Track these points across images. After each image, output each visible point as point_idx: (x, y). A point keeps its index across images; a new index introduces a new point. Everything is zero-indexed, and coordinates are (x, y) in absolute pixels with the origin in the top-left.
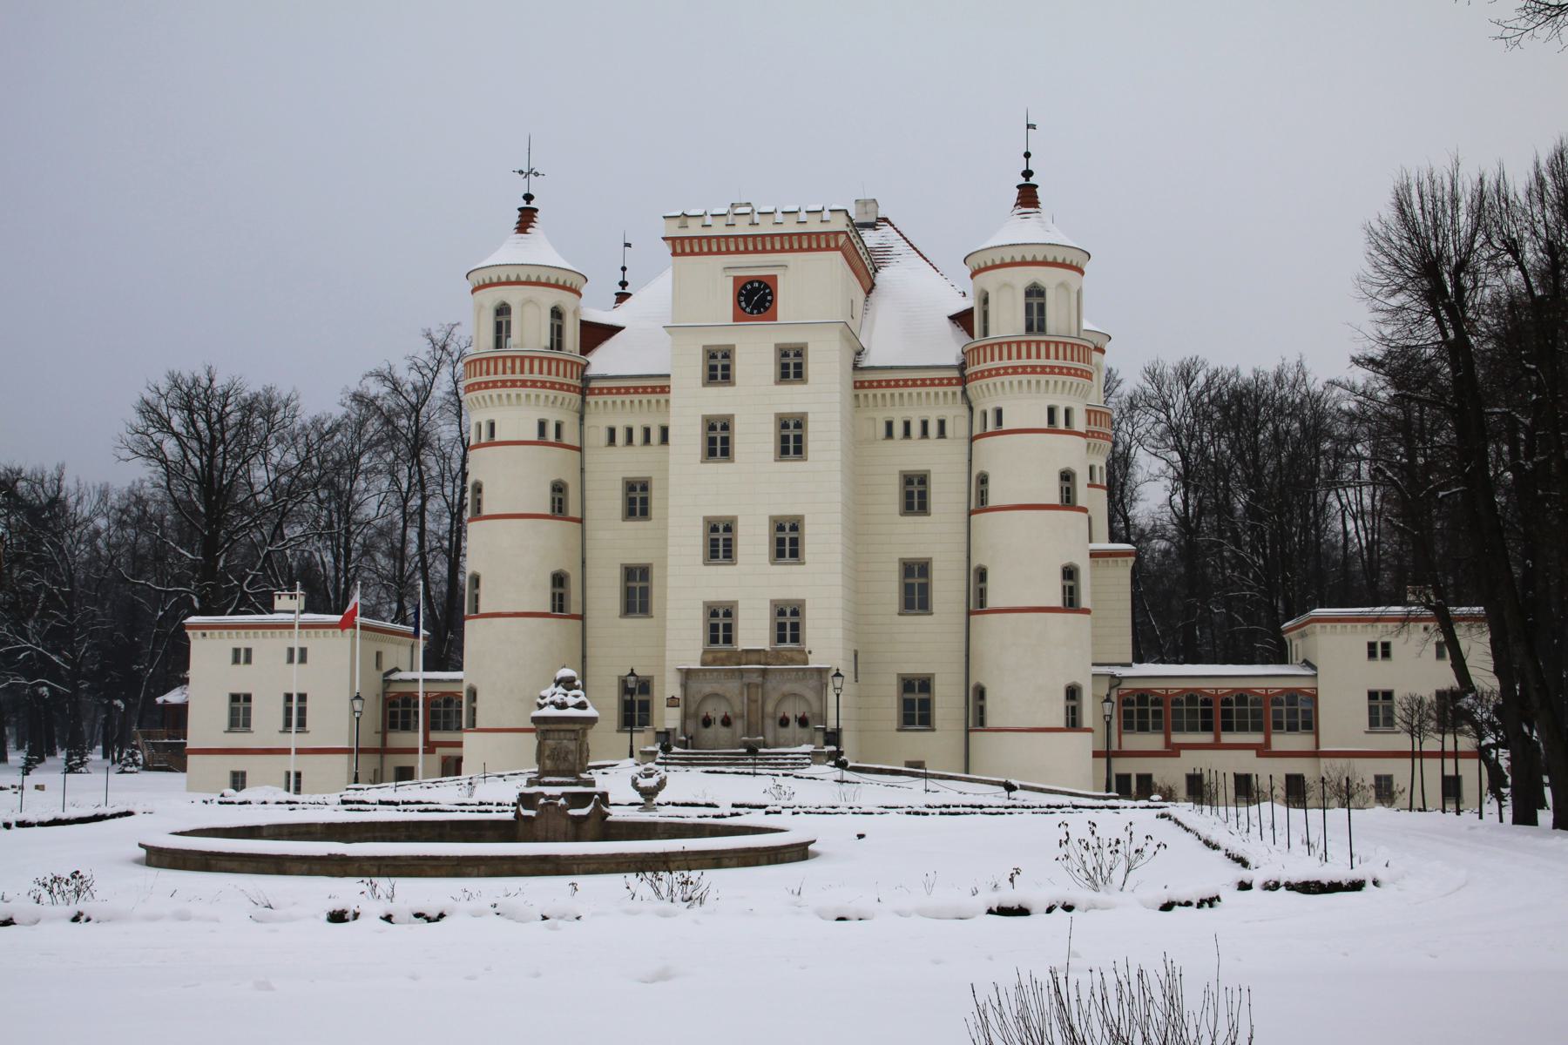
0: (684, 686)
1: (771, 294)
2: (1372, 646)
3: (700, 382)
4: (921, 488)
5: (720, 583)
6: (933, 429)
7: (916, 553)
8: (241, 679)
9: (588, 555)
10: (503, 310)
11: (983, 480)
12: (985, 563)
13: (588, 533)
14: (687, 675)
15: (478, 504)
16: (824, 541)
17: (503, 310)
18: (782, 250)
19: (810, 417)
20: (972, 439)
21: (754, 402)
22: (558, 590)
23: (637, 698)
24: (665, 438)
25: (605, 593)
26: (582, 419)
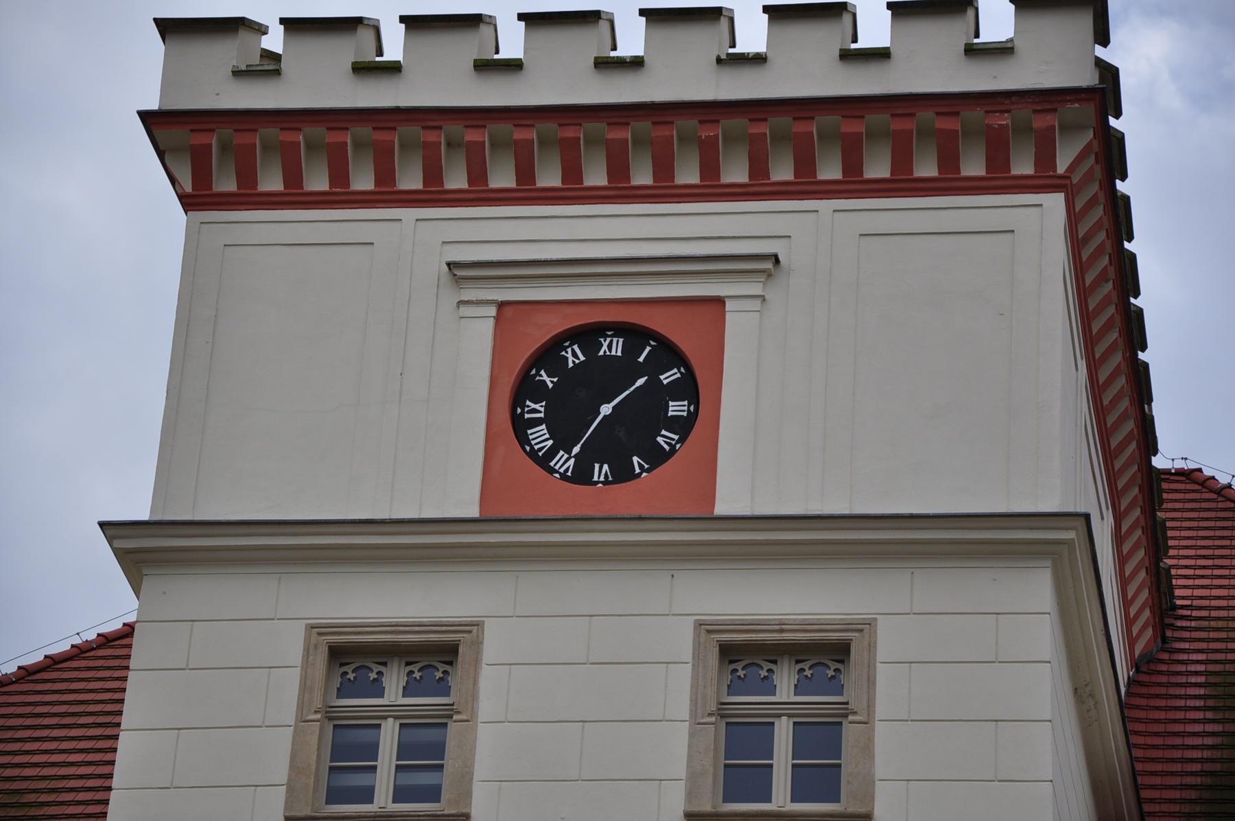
1: (688, 388)
18: (759, 188)
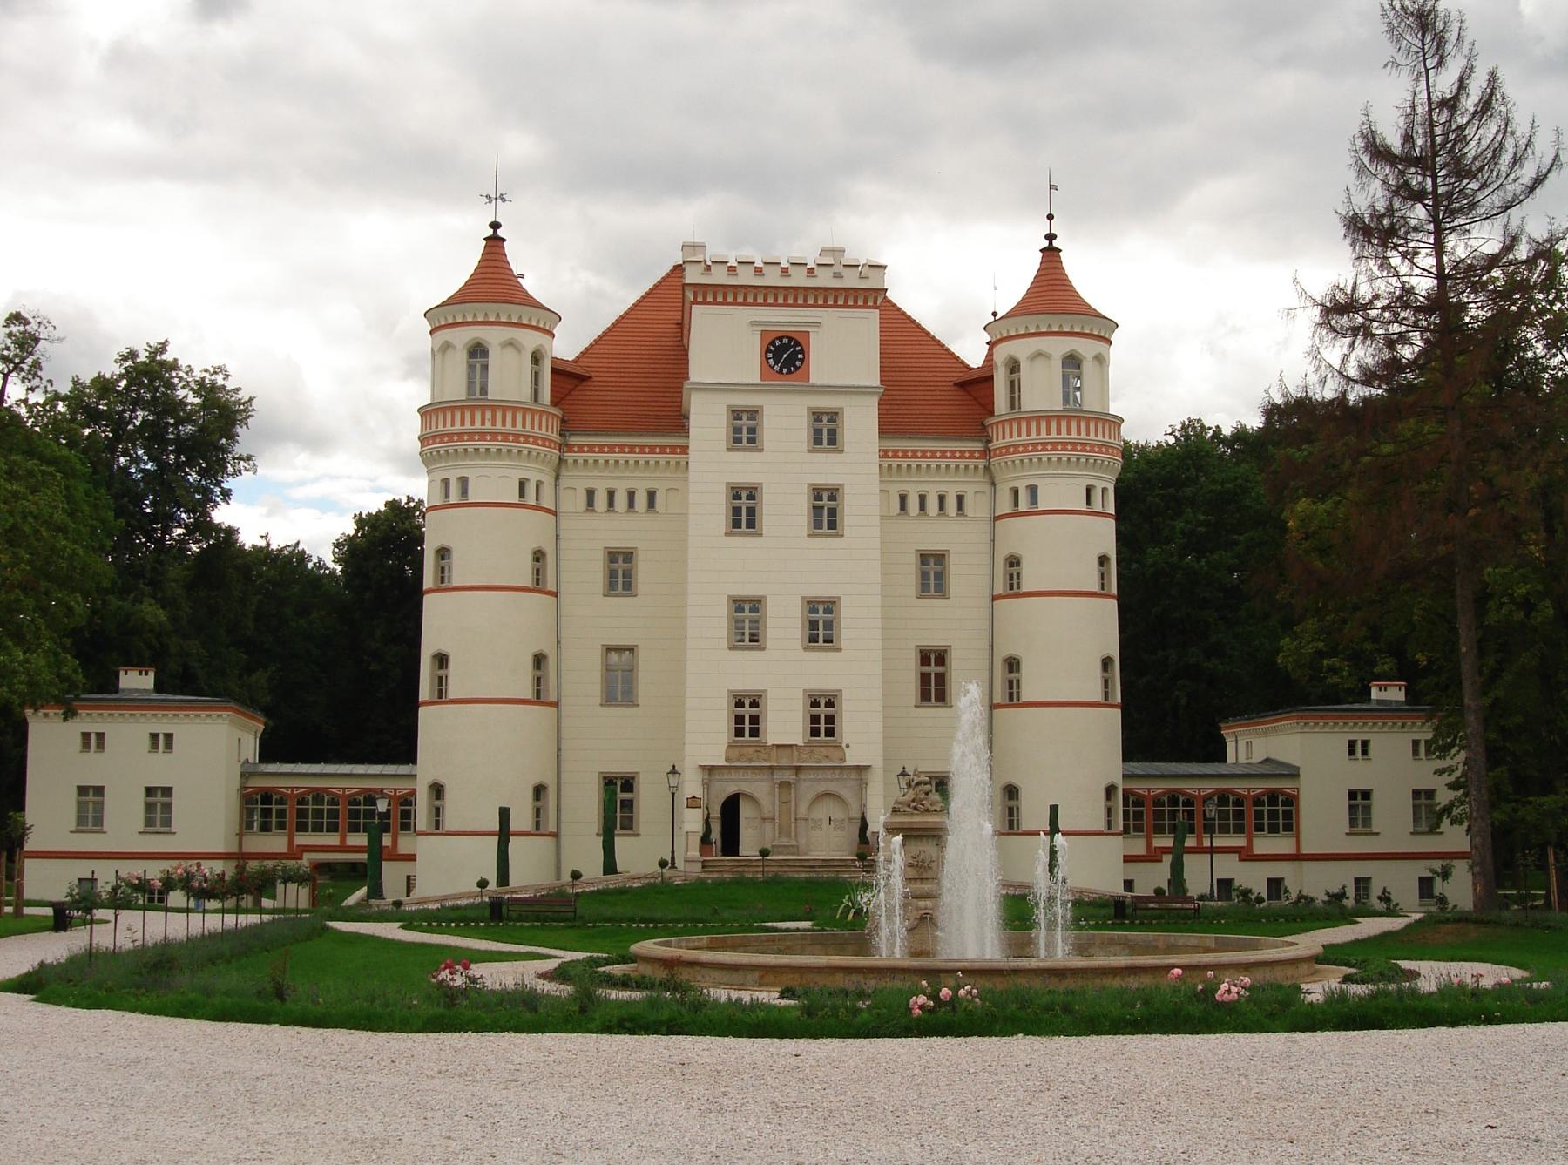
0: (707, 785)
1: (802, 351)
2: (1352, 744)
3: (723, 445)
4: (938, 568)
5: (747, 670)
7: (934, 641)
8: (93, 768)
9: (564, 633)
10: (478, 351)
11: (1013, 562)
12: (1016, 652)
13: (564, 611)
14: (710, 770)
15: (442, 573)
16: (859, 623)
17: (478, 351)
18: (815, 305)
19: (847, 489)
20: (996, 518)
21: (785, 467)
22: (538, 673)
23: (621, 796)
25: (581, 678)
26: (557, 478)
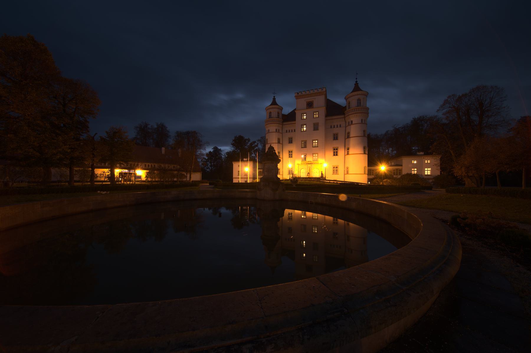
6: (339, 126)
10: (270, 113)
17: (270, 113)
24: (295, 131)
